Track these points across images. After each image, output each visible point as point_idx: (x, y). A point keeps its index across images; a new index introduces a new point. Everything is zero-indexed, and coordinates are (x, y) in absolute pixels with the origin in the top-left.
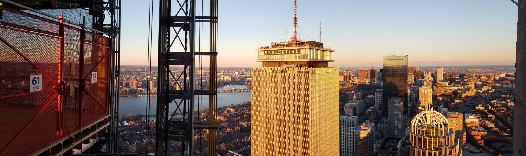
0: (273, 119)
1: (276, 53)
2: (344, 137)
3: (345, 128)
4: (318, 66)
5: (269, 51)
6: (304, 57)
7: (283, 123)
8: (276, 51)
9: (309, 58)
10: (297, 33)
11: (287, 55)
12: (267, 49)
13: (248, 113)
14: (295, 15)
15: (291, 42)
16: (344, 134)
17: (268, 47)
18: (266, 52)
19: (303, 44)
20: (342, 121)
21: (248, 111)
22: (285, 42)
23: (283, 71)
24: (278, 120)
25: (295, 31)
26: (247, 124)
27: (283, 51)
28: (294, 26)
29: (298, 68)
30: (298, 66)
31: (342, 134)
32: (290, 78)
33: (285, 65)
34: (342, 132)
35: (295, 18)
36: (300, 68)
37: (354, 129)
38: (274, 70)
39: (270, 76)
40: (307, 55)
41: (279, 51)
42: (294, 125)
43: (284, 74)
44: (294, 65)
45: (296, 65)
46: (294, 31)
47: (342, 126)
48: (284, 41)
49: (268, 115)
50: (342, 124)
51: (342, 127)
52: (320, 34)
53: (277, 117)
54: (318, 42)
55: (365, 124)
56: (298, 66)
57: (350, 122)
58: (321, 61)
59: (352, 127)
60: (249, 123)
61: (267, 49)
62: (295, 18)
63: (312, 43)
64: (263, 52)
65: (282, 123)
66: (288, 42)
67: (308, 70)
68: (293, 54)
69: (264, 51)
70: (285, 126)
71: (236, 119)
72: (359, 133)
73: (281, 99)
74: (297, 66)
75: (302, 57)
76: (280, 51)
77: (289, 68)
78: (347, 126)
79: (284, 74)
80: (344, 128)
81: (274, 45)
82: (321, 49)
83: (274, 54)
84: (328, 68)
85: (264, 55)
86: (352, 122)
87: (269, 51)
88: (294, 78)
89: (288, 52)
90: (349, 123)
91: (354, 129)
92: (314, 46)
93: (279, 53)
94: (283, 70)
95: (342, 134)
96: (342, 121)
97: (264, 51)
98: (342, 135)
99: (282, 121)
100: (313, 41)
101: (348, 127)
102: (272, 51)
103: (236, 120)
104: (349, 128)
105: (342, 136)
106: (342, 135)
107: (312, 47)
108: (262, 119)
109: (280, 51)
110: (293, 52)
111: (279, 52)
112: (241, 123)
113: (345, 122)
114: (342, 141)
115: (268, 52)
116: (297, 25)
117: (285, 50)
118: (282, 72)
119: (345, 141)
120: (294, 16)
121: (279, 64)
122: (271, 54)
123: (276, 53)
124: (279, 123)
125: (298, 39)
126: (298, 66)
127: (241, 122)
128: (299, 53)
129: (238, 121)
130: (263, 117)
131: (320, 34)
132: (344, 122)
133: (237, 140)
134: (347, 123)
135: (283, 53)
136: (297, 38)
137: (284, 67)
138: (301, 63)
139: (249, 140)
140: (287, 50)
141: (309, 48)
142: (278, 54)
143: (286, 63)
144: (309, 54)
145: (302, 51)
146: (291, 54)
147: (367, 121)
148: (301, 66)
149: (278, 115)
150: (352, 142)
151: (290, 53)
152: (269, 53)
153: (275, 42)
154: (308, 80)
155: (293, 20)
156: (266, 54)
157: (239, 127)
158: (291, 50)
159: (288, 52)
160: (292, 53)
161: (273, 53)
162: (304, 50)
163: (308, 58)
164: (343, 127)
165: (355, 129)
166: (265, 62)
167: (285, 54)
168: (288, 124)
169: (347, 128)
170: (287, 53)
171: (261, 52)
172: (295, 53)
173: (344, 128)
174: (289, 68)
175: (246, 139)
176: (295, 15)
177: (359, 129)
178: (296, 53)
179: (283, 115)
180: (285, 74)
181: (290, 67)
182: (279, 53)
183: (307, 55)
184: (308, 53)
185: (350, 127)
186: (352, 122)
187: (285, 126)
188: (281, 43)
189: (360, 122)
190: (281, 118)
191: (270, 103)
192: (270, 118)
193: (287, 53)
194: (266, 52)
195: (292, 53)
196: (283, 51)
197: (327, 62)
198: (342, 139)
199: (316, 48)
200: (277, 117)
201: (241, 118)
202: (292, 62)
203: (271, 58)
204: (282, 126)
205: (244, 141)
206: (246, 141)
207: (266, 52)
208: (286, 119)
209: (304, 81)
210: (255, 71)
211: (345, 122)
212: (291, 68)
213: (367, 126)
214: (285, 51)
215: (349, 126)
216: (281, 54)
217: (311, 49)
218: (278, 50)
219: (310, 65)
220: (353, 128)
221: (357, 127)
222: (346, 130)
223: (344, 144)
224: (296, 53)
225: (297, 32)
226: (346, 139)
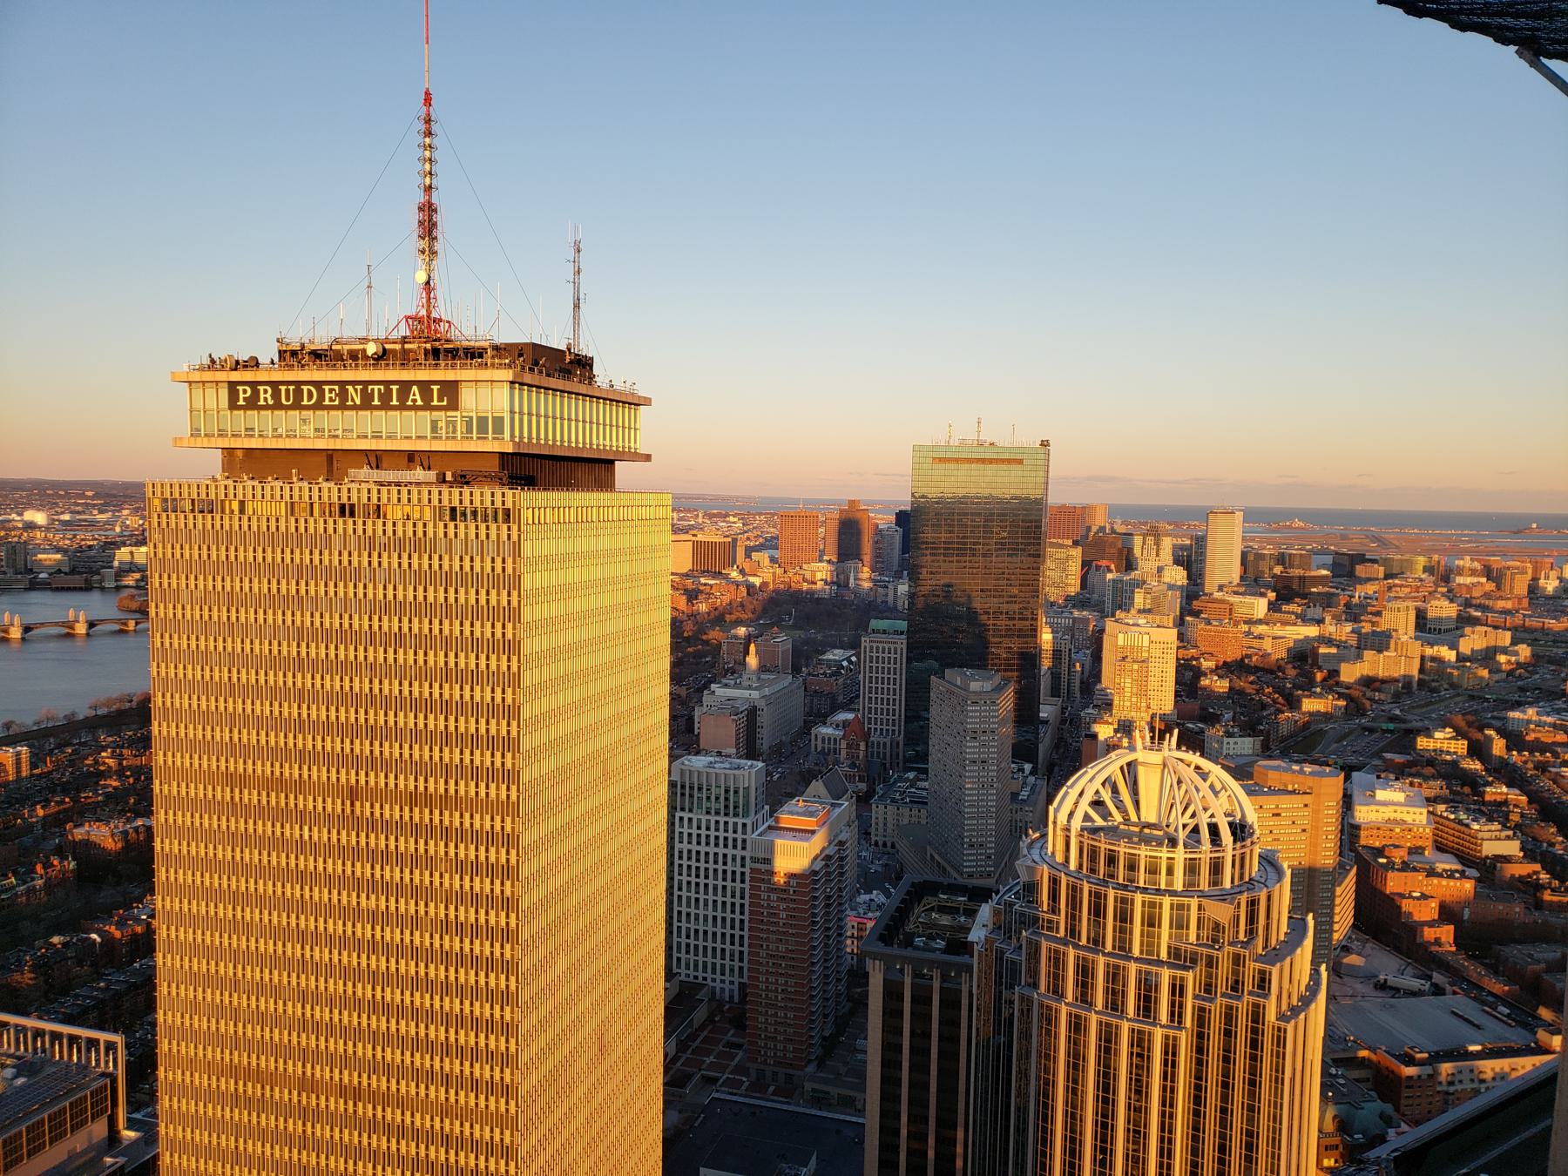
0: (300, 786)
1: (305, 402)
2: (689, 867)
3: (699, 821)
4: (566, 484)
5: (261, 388)
6: (482, 428)
7: (358, 804)
8: (305, 388)
9: (512, 436)
10: (439, 292)
11: (376, 413)
12: (248, 376)
13: (129, 768)
14: (428, 189)
15: (404, 340)
16: (690, 851)
17: (254, 363)
18: (244, 393)
19: (473, 354)
20: (683, 787)
21: (125, 752)
22: (365, 340)
23: (352, 506)
24: (326, 790)
25: (428, 283)
26: (126, 833)
27: (350, 388)
28: (423, 252)
29: (445, 490)
30: (449, 477)
31: (681, 852)
32: (399, 545)
33: (364, 472)
34: (681, 842)
35: (428, 209)
36: (456, 491)
37: (744, 825)
38: (296, 498)
39: (271, 538)
40: (498, 421)
41: (326, 388)
42: (421, 815)
43: (360, 522)
44: (419, 474)
45: (431, 475)
46: (421, 277)
47: (683, 809)
48: (363, 334)
49: (263, 769)
50: (683, 802)
51: (681, 819)
52: (577, 306)
53: (318, 774)
54: (563, 347)
55: (801, 804)
56: (444, 481)
57: (727, 791)
58: (585, 455)
59: (736, 815)
60: (136, 829)
61: (248, 376)
62: (428, 209)
63: (528, 355)
64: (224, 393)
65: (352, 805)
66: (381, 342)
67: (509, 505)
68: (415, 408)
69: (233, 386)
70: (372, 825)
71: (41, 812)
72: (771, 848)
73: (343, 668)
74: (442, 480)
75: (469, 430)
76: (331, 391)
77: (394, 490)
78: (708, 813)
79: (360, 522)
80: (690, 820)
81: (294, 353)
82: (583, 389)
83: (297, 406)
84: (614, 495)
85: (233, 405)
86: (736, 792)
87: (261, 388)
88: (419, 545)
89: (386, 397)
90: (717, 798)
91: (744, 825)
92: (541, 372)
93: (327, 402)
94: (354, 500)
95: (681, 852)
96: (683, 787)
98: (681, 858)
99: (353, 794)
100: (535, 345)
101: (713, 819)
102: (283, 388)
103: (45, 817)
104: (717, 822)
105: (680, 865)
106: (681, 858)
107: (528, 378)
108: (222, 794)
109: (331, 391)
110: (418, 397)
111: (327, 395)
112: (79, 833)
113: (700, 789)
114: (680, 889)
115: (256, 393)
116: (437, 246)
118: (346, 510)
119: (697, 892)
120: (421, 198)
121: (332, 463)
122: (278, 406)
123: (305, 402)
124: (335, 806)
125: (443, 327)
126: (444, 481)
127: (76, 826)
128: (454, 405)
129: (57, 822)
130: (231, 780)
131: (577, 306)
132: (691, 788)
133: (56, 939)
134: (708, 798)
135: (350, 403)
136: (438, 321)
137: (361, 484)
138: (466, 466)
139: (139, 929)
141: (512, 383)
142: (318, 406)
143: (376, 459)
144: (512, 412)
145: (467, 397)
146: (403, 407)
147: (817, 786)
148: (463, 480)
149: (329, 759)
150: (733, 896)
151: (395, 402)
152: (266, 395)
153: (297, 336)
154: (509, 561)
155: (414, 217)
156: (241, 402)
157: (63, 858)
158: (405, 386)
159: (386, 397)
160: (410, 403)
161: (292, 398)
162: (484, 391)
163: (507, 435)
164: (686, 815)
165: (749, 828)
166: (240, 454)
167: (366, 404)
168: (392, 812)
169: (708, 821)
170: (376, 402)
171: (211, 392)
172: (427, 406)
173: (690, 820)
174: (394, 490)
175: (121, 924)
176: (428, 189)
177: (770, 827)
178: (435, 403)
179: (355, 762)
180: (369, 523)
181: (398, 484)
182: (327, 402)
183: (498, 421)
184: (507, 407)
185: (726, 814)
186: (736, 792)
187: (372, 825)
188: (336, 341)
189: (776, 796)
190: (347, 777)
191: (275, 694)
192: (281, 784)
193: (376, 402)
194: (240, 388)
195: (410, 403)
196: (350, 388)
197: (612, 462)
198: (680, 882)
199: (553, 382)
200: (318, 774)
201: (75, 800)
202: (411, 458)
203: (275, 430)
204: (352, 822)
205: (108, 940)
206: (118, 934)
207: (244, 393)
208: (377, 780)
209: (483, 565)
210: (170, 505)
211: (700, 789)
212: (404, 490)
213: (811, 814)
214: (364, 391)
215: (717, 813)
216: (343, 407)
217: (521, 384)
218: (319, 385)
219: (517, 478)
220: (740, 821)
221: (760, 816)
222: (703, 832)
223: (688, 905)
224: (435, 403)
225: (438, 287)
226: (702, 881)
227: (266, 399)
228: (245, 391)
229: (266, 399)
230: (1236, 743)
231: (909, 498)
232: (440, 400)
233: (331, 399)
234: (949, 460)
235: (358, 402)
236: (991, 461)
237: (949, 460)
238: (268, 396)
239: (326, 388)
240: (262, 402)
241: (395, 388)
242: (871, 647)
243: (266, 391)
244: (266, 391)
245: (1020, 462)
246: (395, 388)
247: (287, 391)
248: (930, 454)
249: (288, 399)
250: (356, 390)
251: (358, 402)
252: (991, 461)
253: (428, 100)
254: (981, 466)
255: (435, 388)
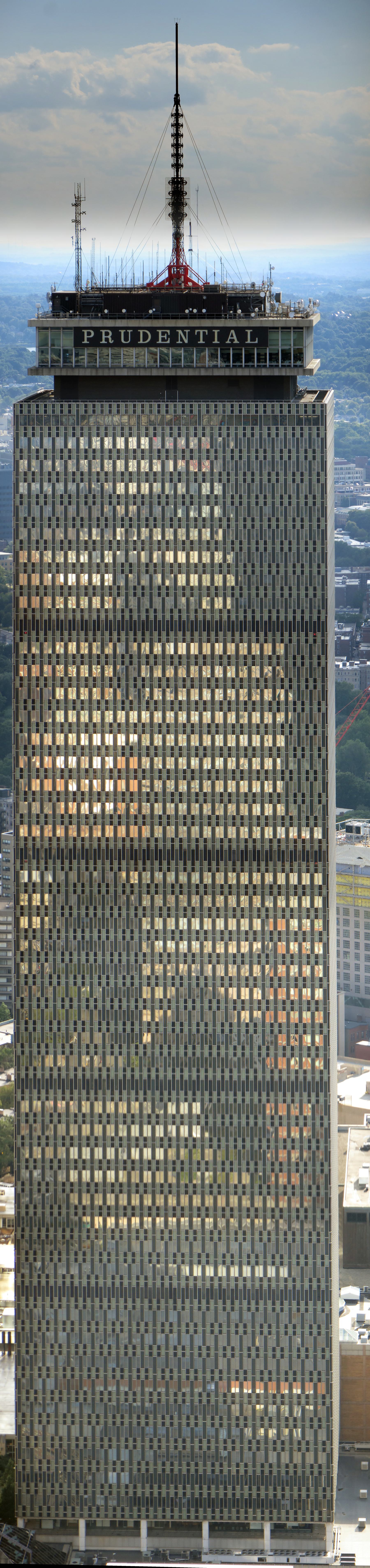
1: (141, 342)
8: (141, 332)
27: (180, 332)
41: (160, 332)
93: (160, 342)
97: (78, 332)
102: (122, 332)
110: (235, 337)
111: (160, 336)
117: (193, 329)
120: (172, 173)
123: (141, 342)
140: (201, 332)
142: (153, 343)
151: (216, 341)
156: (86, 342)
170: (201, 342)
176: (177, 166)
178: (249, 342)
182: (160, 342)
193: (201, 342)
194: (85, 331)
196: (180, 332)
224: (249, 342)
227: (107, 340)
228: (89, 334)
229: (107, 340)
232: (253, 339)
233: (163, 339)
235: (186, 341)
238: (109, 337)
239: (160, 332)
240: (104, 342)
241: (216, 332)
243: (107, 334)
244: (107, 334)
246: (216, 332)
247: (126, 334)
249: (126, 339)
250: (185, 334)
251: (186, 341)
253: (177, 102)
255: (249, 332)
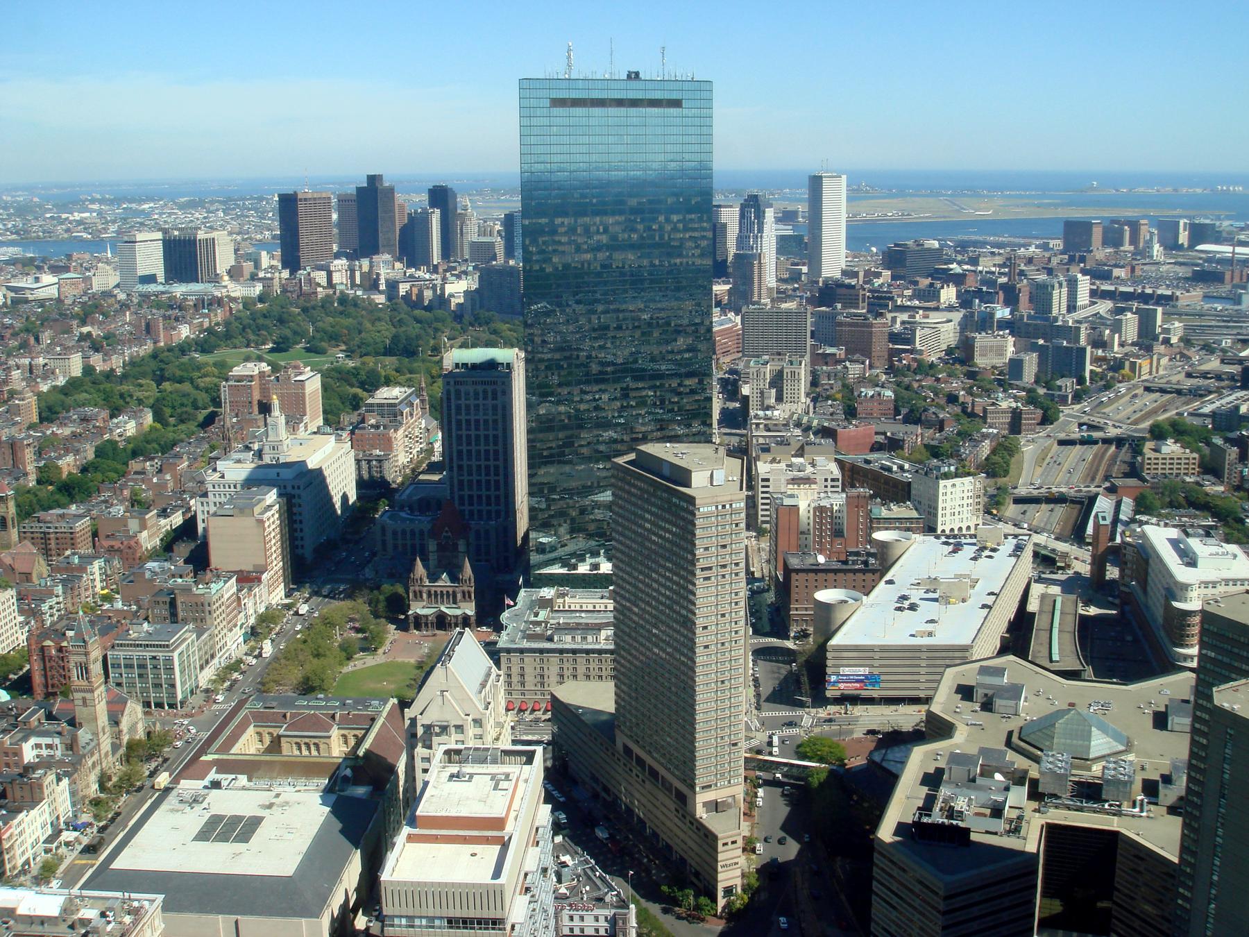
230: (954, 485)
231: (516, 169)
234: (576, 103)
236: (634, 103)
237: (576, 103)
242: (458, 393)
245: (676, 103)
248: (545, 93)
252: (634, 103)
254: (622, 111)
